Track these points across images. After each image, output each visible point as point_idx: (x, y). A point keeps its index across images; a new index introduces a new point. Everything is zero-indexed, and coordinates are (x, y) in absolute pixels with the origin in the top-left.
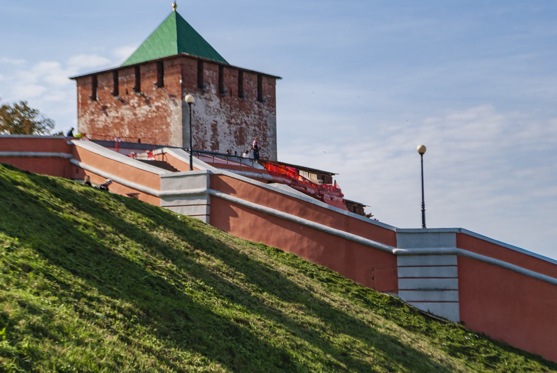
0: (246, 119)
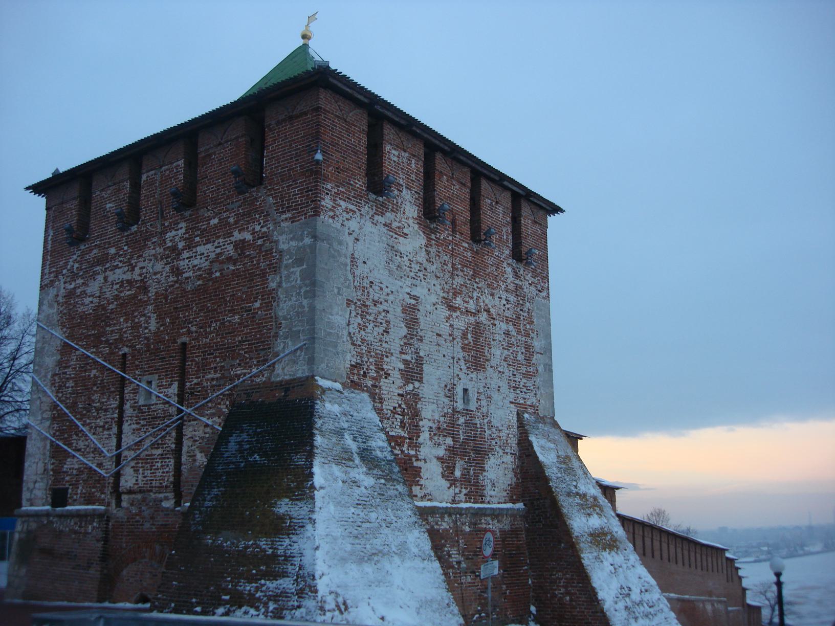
0: (488, 300)
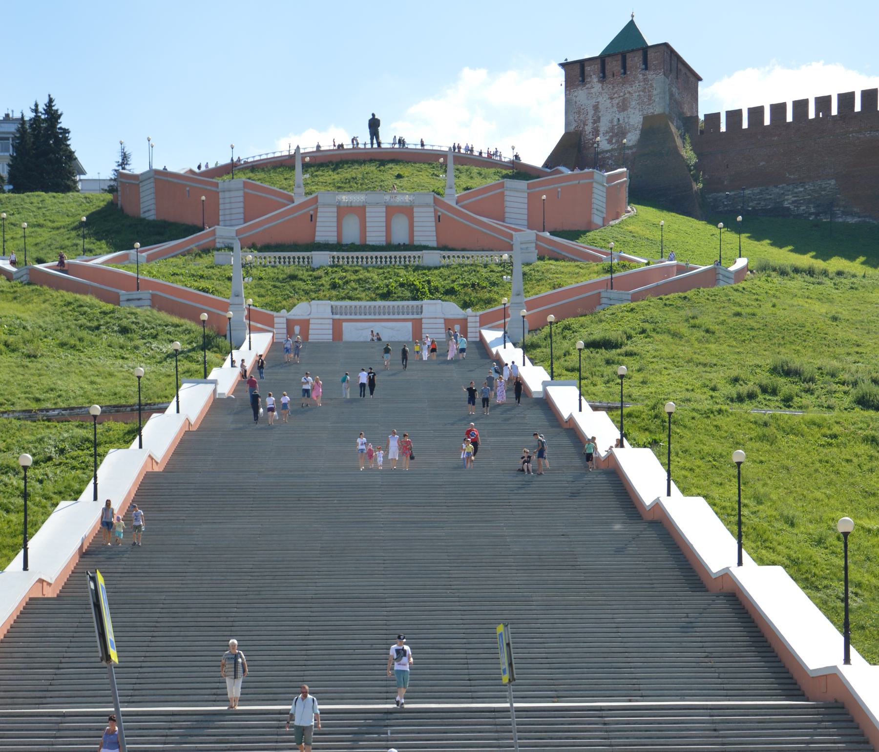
0: (630, 89)
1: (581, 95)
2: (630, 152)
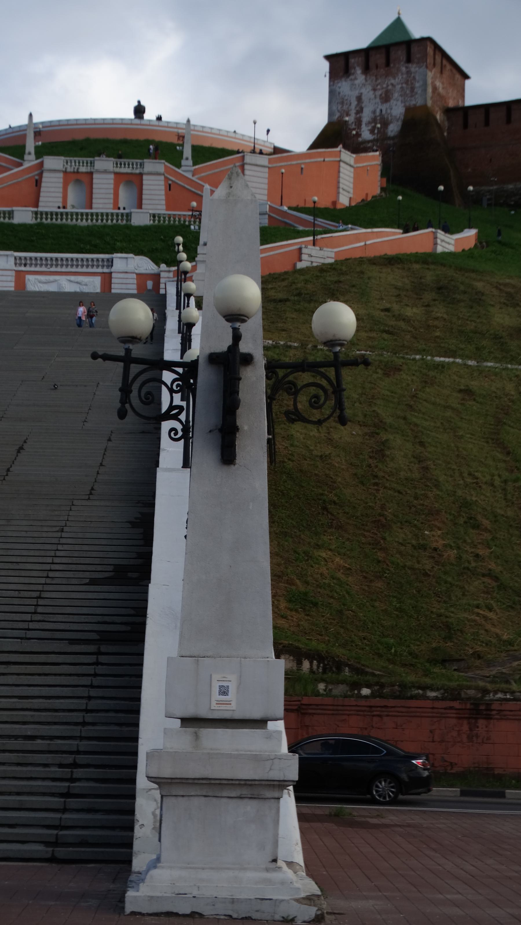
0: (393, 81)
1: (344, 87)
2: (391, 142)
